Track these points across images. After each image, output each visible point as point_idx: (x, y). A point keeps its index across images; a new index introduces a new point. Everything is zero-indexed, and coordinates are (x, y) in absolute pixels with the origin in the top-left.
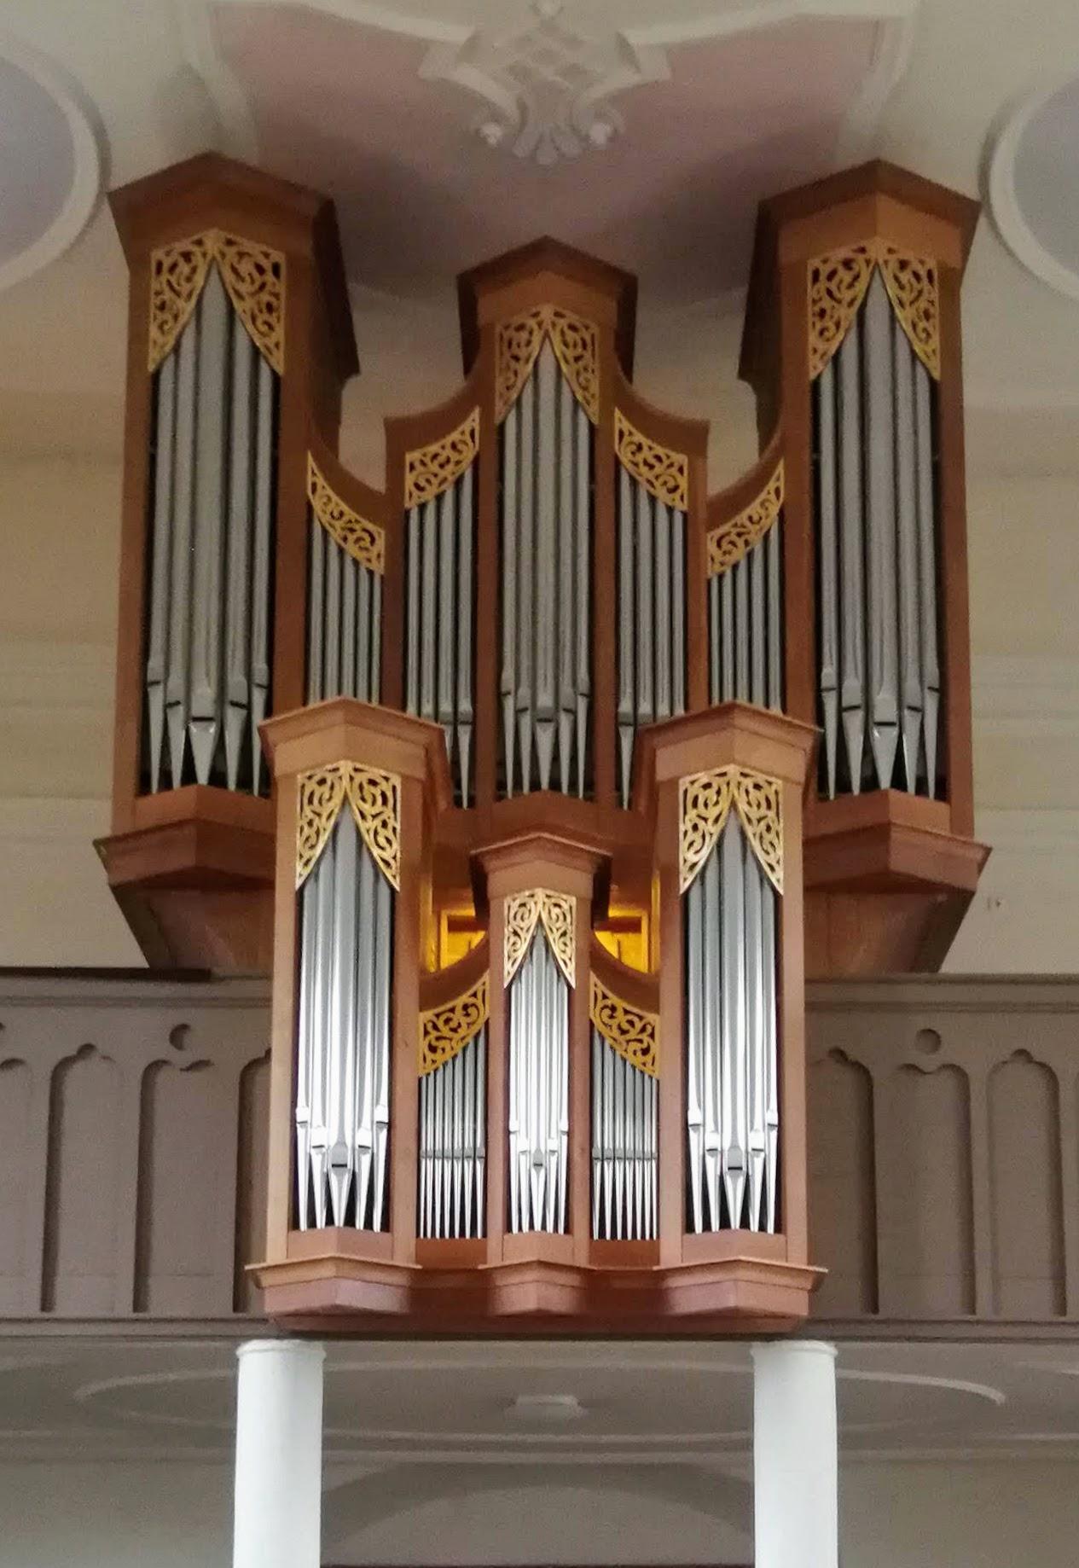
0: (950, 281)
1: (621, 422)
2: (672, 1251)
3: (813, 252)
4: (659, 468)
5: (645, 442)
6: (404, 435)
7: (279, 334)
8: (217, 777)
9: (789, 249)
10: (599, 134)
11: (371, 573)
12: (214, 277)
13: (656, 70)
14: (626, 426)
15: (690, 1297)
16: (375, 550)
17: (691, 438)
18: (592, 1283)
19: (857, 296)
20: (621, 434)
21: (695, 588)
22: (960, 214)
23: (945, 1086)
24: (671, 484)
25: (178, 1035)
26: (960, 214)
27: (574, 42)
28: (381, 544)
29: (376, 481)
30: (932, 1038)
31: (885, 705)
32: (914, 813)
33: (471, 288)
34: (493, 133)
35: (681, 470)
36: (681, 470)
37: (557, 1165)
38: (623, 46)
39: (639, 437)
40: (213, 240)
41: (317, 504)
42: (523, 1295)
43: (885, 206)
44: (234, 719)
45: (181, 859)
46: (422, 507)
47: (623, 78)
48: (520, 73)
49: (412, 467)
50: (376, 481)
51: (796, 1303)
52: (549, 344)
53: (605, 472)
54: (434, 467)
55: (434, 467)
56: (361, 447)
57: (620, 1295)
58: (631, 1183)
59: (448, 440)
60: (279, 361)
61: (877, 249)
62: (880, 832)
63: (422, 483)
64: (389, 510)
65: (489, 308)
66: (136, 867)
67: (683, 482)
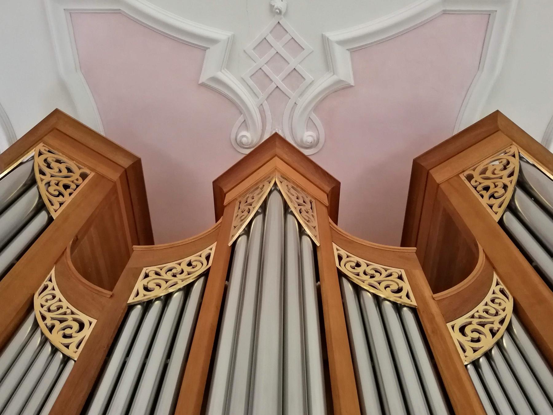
1: (337, 250)
4: (378, 277)
5: (361, 261)
7: (68, 200)
11: (66, 359)
12: (30, 164)
13: (344, 70)
14: (343, 253)
16: (78, 337)
20: (340, 258)
24: (395, 287)
27: (295, 45)
28: (87, 332)
35: (400, 277)
36: (400, 277)
38: (325, 42)
39: (355, 259)
41: (37, 301)
46: (147, 305)
47: (324, 81)
48: (261, 76)
49: (147, 276)
54: (169, 276)
55: (169, 276)
59: (187, 260)
63: (151, 285)
67: (406, 286)
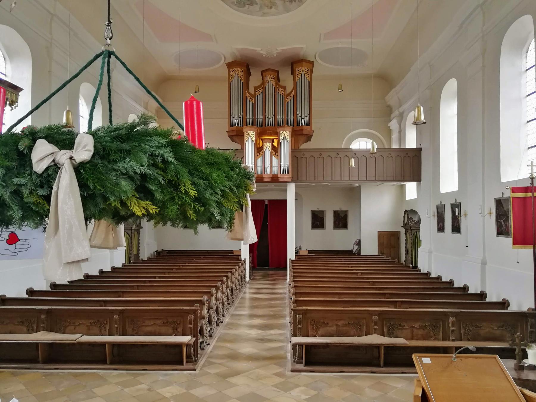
0: (311, 71)
2: (279, 176)
3: (297, 68)
6: (255, 88)
8: (238, 124)
9: (294, 67)
10: (275, 55)
15: (281, 180)
17: (285, 88)
18: (272, 178)
19: (302, 71)
21: (285, 104)
22: (312, 63)
23: (305, 159)
25: (235, 155)
26: (312, 63)
29: (252, 93)
30: (304, 154)
31: (303, 116)
32: (306, 128)
33: (262, 72)
34: (264, 56)
37: (269, 168)
40: (236, 69)
42: (266, 180)
43: (304, 63)
44: (239, 119)
45: (235, 134)
50: (252, 93)
51: (290, 180)
52: (270, 79)
53: (276, 92)
56: (252, 90)
57: (275, 179)
58: (276, 169)
60: (243, 81)
61: (303, 68)
62: (302, 130)
64: (254, 96)
65: (264, 74)
66: (231, 134)
